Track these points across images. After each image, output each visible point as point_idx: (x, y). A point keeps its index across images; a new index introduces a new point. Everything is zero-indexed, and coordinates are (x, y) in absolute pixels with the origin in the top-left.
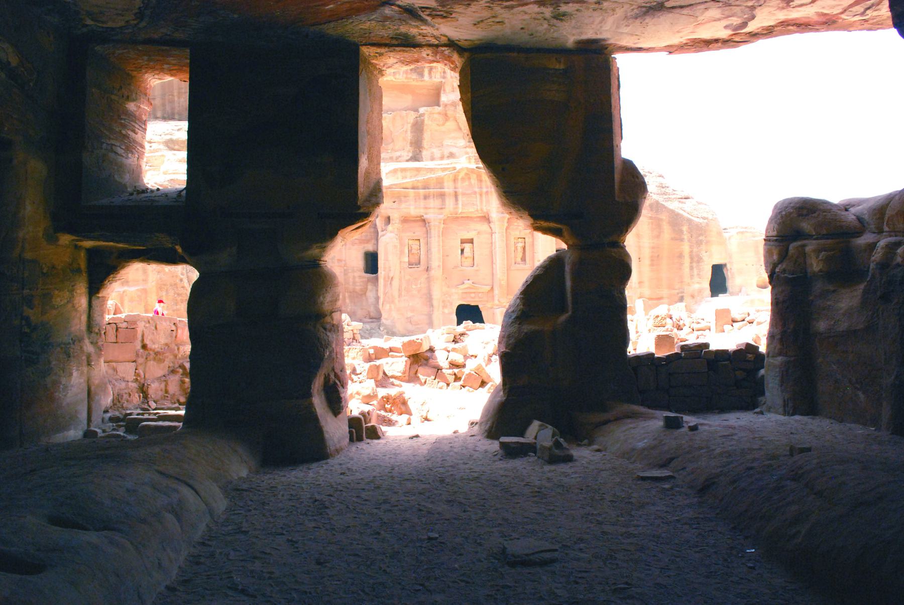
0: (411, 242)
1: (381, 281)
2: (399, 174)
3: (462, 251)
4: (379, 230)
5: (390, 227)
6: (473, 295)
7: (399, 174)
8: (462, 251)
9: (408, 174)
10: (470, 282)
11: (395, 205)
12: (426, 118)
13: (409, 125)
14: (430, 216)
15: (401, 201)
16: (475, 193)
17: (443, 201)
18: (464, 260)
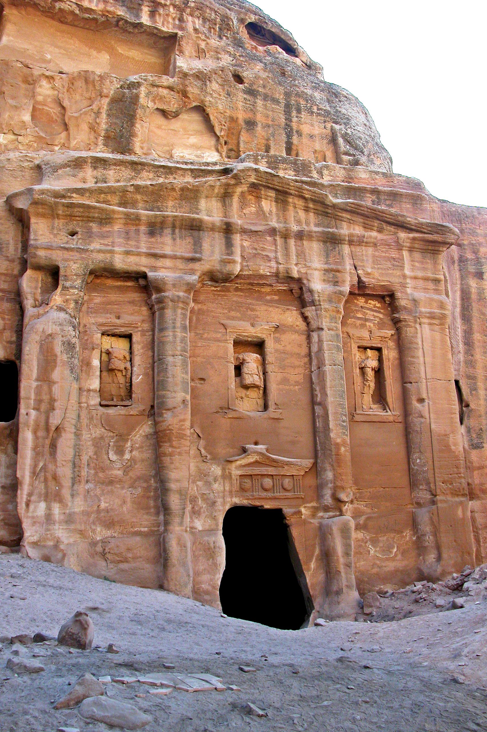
0: (108, 343)
1: (27, 437)
2: (89, 173)
3: (238, 370)
4: (28, 303)
5: (57, 298)
7: (89, 173)
8: (238, 370)
9: (111, 173)
10: (261, 448)
11: (74, 243)
12: (143, 91)
13: (106, 101)
14: (164, 273)
15: (89, 235)
16: (273, 232)
17: (197, 244)
18: (243, 392)
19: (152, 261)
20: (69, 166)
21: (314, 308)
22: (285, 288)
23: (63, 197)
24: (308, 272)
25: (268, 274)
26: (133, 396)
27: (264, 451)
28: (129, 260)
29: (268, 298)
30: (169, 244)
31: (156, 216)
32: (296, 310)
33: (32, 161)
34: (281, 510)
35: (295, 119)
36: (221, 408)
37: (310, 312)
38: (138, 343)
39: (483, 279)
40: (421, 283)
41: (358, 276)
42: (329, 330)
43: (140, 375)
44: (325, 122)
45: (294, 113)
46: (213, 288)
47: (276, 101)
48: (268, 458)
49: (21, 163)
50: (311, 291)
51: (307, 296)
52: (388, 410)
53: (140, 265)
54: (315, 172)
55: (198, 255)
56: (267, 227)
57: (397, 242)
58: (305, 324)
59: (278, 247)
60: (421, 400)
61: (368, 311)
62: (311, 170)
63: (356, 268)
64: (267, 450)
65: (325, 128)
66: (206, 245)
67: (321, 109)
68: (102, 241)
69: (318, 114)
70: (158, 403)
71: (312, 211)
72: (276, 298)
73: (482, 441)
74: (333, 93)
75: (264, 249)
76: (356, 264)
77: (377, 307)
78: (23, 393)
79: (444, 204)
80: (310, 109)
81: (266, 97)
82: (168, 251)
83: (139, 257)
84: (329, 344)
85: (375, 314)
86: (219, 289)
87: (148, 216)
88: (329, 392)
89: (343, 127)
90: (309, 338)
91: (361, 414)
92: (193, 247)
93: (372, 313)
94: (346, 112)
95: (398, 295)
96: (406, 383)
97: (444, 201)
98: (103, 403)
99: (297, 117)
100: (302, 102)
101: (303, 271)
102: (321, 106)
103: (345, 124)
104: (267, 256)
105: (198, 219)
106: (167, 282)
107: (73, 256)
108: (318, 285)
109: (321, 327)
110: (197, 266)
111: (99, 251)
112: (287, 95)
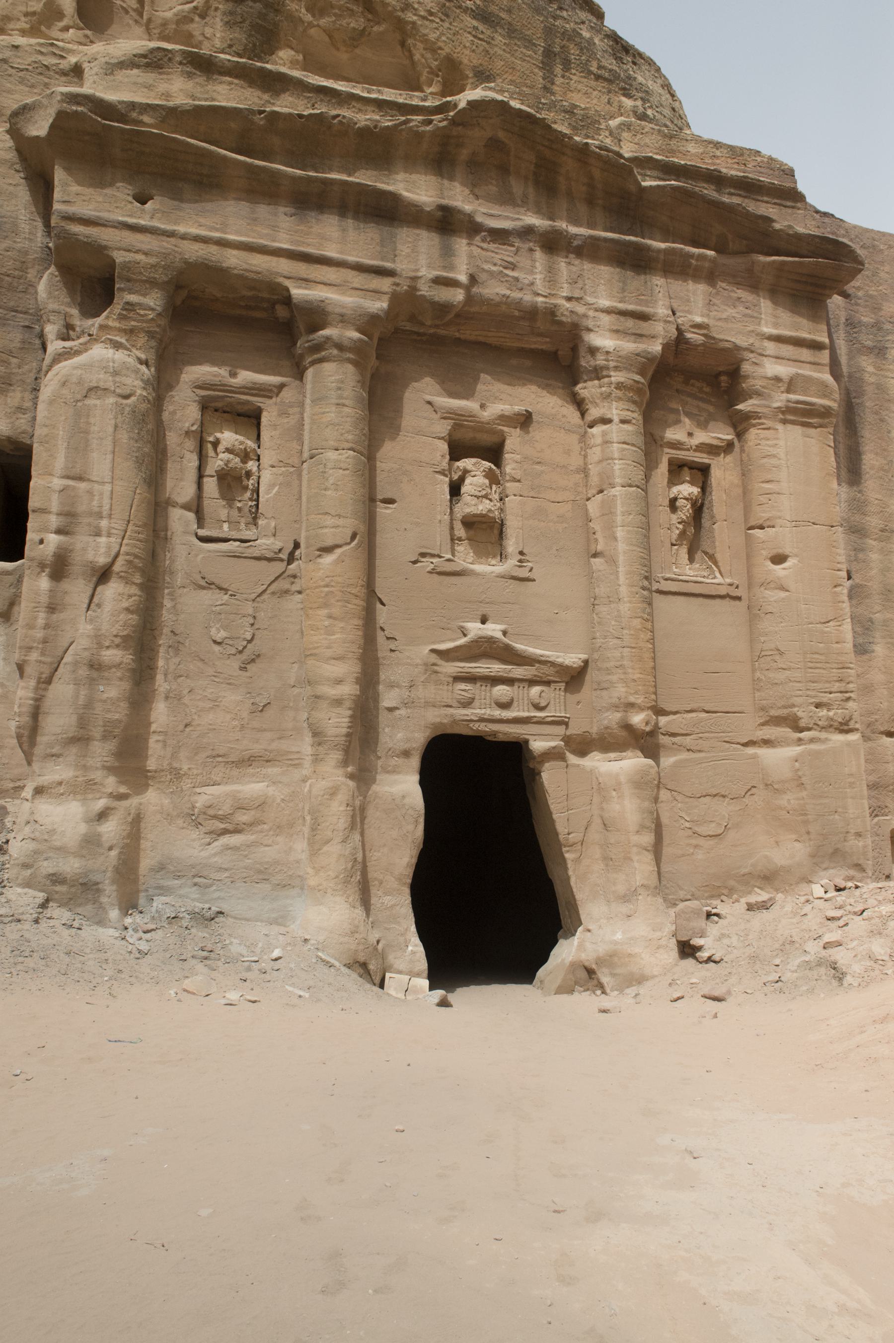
6: (501, 691)
19: (302, 269)
20: (138, 67)
21: (596, 382)
22: (544, 347)
23: (122, 118)
24: (591, 313)
25: (517, 313)
26: (260, 522)
27: (499, 635)
28: (255, 262)
29: (514, 362)
30: (332, 236)
31: (310, 179)
32: (563, 388)
33: (62, 57)
34: (527, 742)
35: (559, 81)
36: (423, 555)
37: (587, 389)
38: (275, 426)
39: (885, 359)
40: (787, 350)
41: (678, 329)
42: (623, 422)
43: (274, 485)
44: (609, 92)
45: (558, 70)
46: (415, 337)
47: (530, 43)
48: (508, 648)
49: (40, 58)
50: (593, 351)
51: (585, 362)
52: (718, 575)
53: (277, 273)
54: (607, 133)
55: (388, 265)
56: (519, 224)
57: (750, 271)
58: (578, 414)
59: (537, 264)
60: (779, 559)
61: (689, 399)
62: (599, 129)
63: (674, 313)
64: (505, 633)
65: (609, 103)
66: (404, 249)
67: (604, 68)
68: (202, 220)
69: (598, 77)
70: (307, 538)
71: (600, 202)
72: (528, 363)
73: (871, 640)
74: (621, 48)
75: (513, 267)
76: (675, 306)
77: (706, 393)
78: (34, 501)
79: (826, 220)
80: (586, 64)
81: (512, 32)
82: (331, 252)
83: (275, 259)
84: (624, 450)
85: (701, 404)
86: (424, 338)
87: (294, 179)
88: (620, 533)
89: (639, 103)
90: (583, 437)
91: (672, 580)
92: (378, 248)
93: (695, 402)
94: (644, 82)
95: (746, 368)
96: (751, 528)
97: (825, 214)
98: (202, 532)
99: (563, 77)
100: (574, 50)
101: (580, 309)
102: (605, 63)
103: (642, 99)
104: (517, 279)
105: (390, 193)
106: (329, 309)
107: (142, 242)
109: (609, 416)
110: (385, 284)
111: (197, 239)
112: (549, 31)
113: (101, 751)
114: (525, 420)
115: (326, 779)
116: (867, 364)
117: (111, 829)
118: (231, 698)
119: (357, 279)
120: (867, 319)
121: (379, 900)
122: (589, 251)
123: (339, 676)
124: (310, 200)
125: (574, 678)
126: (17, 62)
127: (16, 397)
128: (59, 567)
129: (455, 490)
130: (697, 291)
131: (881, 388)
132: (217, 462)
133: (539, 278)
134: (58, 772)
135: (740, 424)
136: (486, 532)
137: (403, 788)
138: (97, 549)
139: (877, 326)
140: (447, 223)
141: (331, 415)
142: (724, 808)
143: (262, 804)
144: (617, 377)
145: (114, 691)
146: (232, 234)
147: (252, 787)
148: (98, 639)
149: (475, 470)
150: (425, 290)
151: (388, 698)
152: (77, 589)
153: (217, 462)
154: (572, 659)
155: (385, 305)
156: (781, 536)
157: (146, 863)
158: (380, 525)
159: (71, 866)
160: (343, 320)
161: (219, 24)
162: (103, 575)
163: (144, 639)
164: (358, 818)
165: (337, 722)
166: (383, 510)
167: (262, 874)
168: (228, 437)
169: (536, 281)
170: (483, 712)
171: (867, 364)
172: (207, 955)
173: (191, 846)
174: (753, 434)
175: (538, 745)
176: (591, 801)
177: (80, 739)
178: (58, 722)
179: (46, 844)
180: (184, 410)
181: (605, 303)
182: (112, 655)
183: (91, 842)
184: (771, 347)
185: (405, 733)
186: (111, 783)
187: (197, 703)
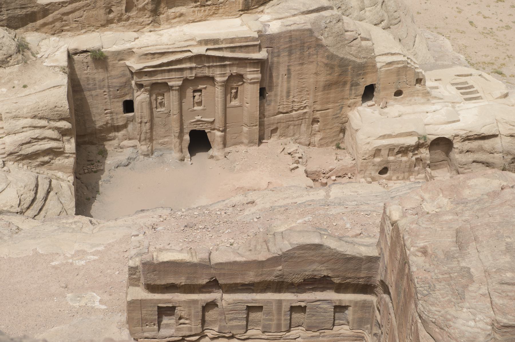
6: (201, 125)
30: (173, 75)
108: (218, 79)
110: (182, 79)
113: (148, 140)
114: (205, 88)
115: (176, 141)
116: (275, 59)
117: (150, 148)
118: (163, 130)
119: (178, 79)
120: (276, 51)
121: (184, 150)
122: (216, 66)
123: (177, 130)
124: (170, 71)
125: (212, 123)
126: (125, 52)
127: (130, 95)
128: (141, 123)
129: (194, 97)
130: (235, 68)
131: (278, 63)
132: (159, 101)
133: (207, 71)
134: (143, 143)
135: (244, 82)
136: (200, 103)
137: (187, 137)
138: (145, 120)
139: (279, 52)
140: (191, 69)
141: (175, 98)
142: (236, 135)
143: (168, 142)
144: (220, 84)
145: (148, 135)
146: (159, 78)
147: (166, 140)
148: (146, 130)
149: (197, 94)
150: (188, 78)
151: (185, 127)
152: (143, 124)
153: (159, 101)
154: (211, 120)
155: (181, 82)
156: (248, 100)
157: (154, 149)
158: (183, 106)
159: (146, 153)
160: (176, 87)
161: (150, 5)
162: (146, 123)
163: (151, 128)
164: (181, 143)
165: (177, 135)
166: (183, 104)
167: (168, 149)
168: (160, 98)
169: (207, 72)
170: (198, 128)
171: (275, 59)
172: (163, 162)
173: (159, 147)
174: (245, 84)
175: (206, 131)
176: (215, 136)
177: (145, 140)
178: (143, 138)
179: (143, 151)
180: (154, 97)
181: (218, 73)
182: (148, 131)
183: (148, 150)
184: (248, 73)
185: (187, 130)
186: (149, 143)
187: (159, 131)
